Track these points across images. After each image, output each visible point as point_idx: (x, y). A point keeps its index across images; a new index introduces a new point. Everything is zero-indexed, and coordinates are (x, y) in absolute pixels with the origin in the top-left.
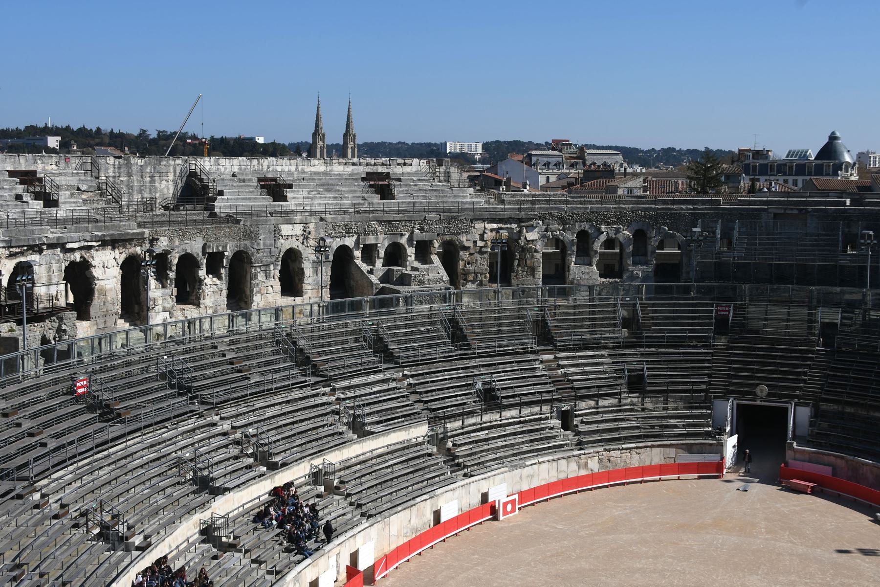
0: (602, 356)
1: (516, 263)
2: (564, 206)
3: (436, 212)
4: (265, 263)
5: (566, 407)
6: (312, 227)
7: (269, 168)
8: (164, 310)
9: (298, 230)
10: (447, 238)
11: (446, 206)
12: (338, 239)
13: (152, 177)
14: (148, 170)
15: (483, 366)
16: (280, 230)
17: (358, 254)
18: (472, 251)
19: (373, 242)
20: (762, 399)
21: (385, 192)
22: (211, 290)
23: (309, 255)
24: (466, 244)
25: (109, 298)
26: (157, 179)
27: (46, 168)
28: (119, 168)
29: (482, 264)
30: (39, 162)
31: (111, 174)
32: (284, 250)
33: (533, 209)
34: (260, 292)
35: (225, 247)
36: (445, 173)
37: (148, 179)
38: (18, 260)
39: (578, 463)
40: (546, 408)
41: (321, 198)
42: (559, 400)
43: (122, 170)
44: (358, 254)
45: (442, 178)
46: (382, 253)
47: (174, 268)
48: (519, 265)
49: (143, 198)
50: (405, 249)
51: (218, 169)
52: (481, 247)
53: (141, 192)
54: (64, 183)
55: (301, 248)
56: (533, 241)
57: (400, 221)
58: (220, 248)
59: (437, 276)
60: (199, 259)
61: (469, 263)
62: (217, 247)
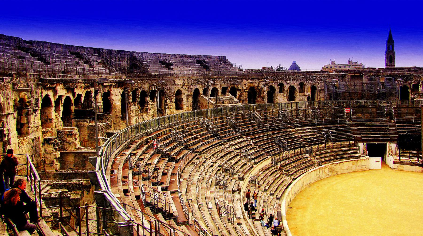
1: (257, 96)
6: (186, 80)
8: (136, 116)
9: (181, 82)
10: (233, 86)
11: (230, 73)
13: (119, 59)
16: (175, 82)
17: (201, 92)
18: (242, 91)
23: (185, 93)
24: (240, 88)
25: (117, 110)
32: (176, 90)
44: (201, 92)
47: (139, 97)
55: (182, 89)
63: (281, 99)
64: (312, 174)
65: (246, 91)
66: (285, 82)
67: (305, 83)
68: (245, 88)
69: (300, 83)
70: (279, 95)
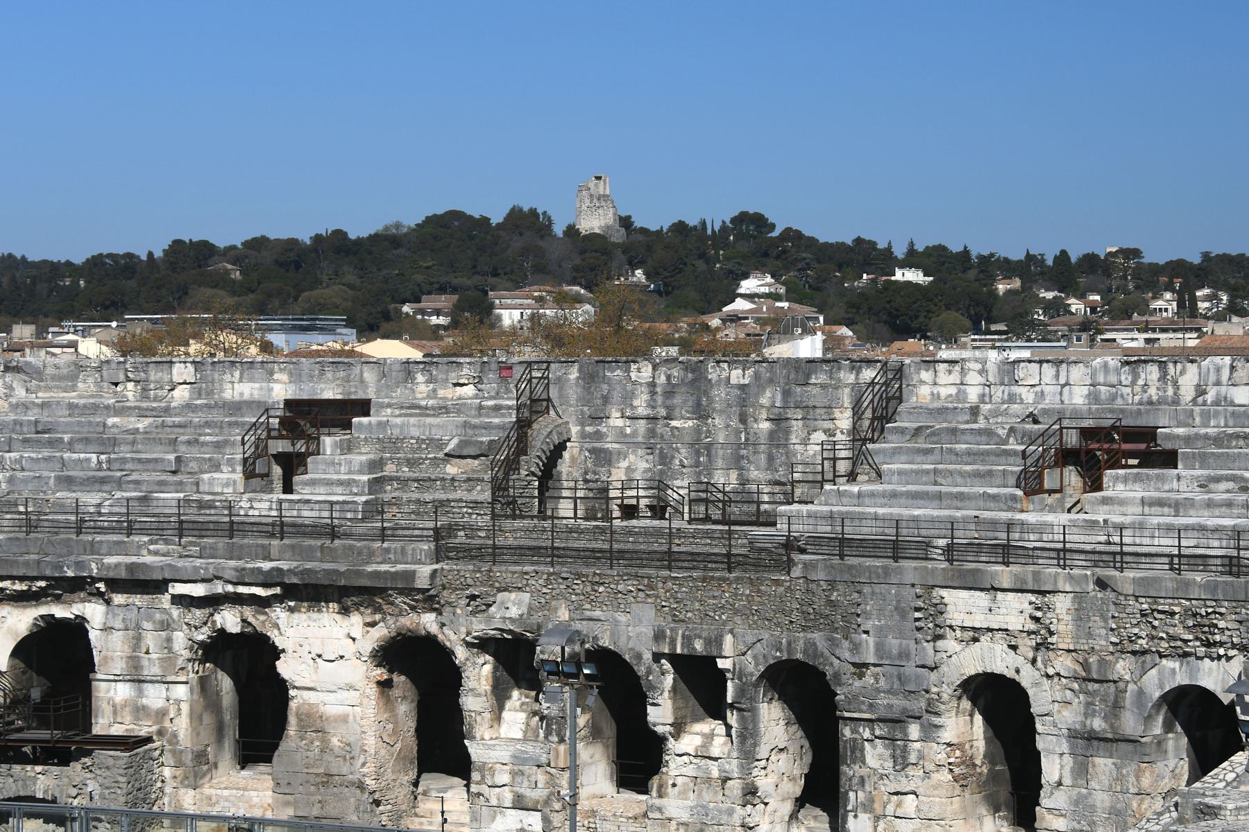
4: (883, 713)
7: (1200, 391)
12: (1168, 664)
14: (764, 401)
22: (690, 771)
25: (335, 741)
26: (797, 426)
27: (441, 393)
28: (669, 393)
30: (420, 378)
31: (642, 411)
34: (868, 807)
35: (719, 642)
37: (765, 426)
38: (43, 610)
41: (1210, 504)
43: (677, 400)
49: (743, 481)
51: (1012, 399)
53: (737, 462)
54: (415, 432)
55: (1028, 678)
58: (699, 646)
60: (641, 670)
62: (688, 640)
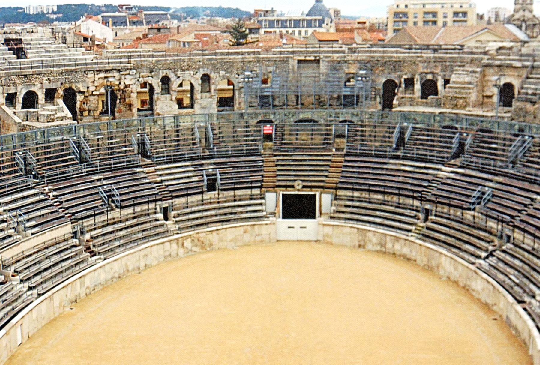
0: (187, 166)
1: (118, 101)
2: (150, 59)
3: (59, 66)
5: (165, 204)
10: (68, 85)
15: (105, 179)
18: (86, 94)
19: (14, 92)
20: (298, 190)
21: (20, 53)
24: (82, 90)
29: (96, 104)
33: (129, 63)
36: (62, 37)
39: (178, 243)
40: (152, 206)
42: (160, 200)
45: (60, 42)
46: (20, 100)
48: (120, 102)
50: (37, 95)
52: (93, 92)
56: (129, 85)
57: (32, 75)
59: (63, 114)
61: (84, 103)
63: (165, 106)
64: (154, 250)
65: (94, 93)
66: (173, 75)
67: (212, 75)
68: (92, 88)
69: (204, 75)
70: (163, 98)
